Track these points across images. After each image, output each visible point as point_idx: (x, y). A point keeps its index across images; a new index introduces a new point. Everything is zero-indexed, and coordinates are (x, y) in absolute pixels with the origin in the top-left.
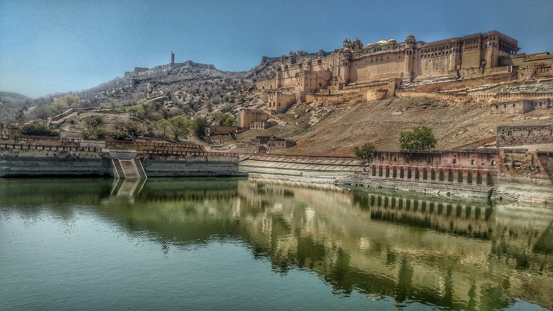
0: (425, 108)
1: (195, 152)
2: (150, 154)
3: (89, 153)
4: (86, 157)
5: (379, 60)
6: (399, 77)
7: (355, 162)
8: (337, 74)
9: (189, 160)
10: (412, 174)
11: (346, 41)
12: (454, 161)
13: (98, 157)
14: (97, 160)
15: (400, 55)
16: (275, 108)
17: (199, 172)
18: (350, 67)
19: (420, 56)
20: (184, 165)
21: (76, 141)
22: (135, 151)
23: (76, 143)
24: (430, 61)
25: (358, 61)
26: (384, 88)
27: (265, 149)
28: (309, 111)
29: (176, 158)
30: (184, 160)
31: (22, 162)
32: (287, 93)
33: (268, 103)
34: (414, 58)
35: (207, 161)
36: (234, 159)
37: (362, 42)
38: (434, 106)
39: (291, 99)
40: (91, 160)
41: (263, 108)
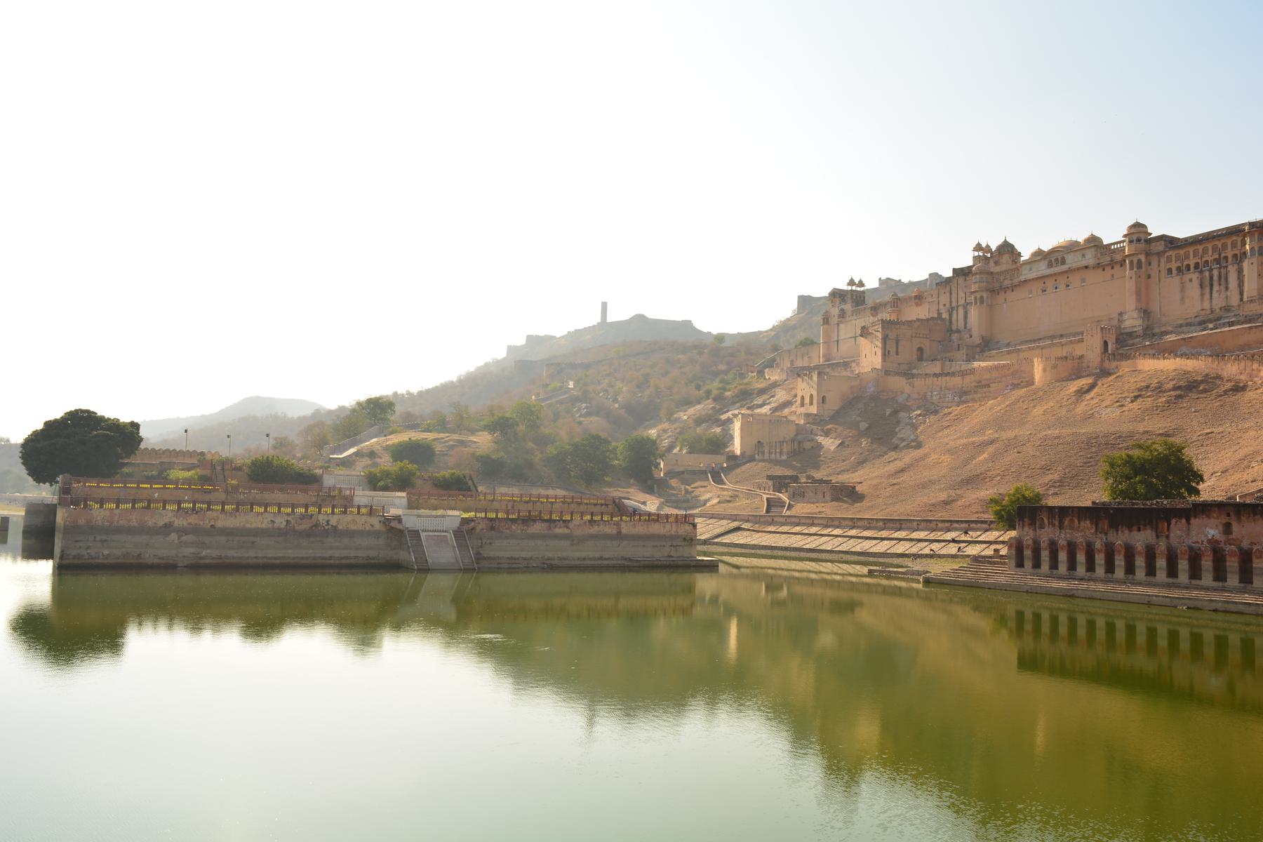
0: (1180, 397)
1: (592, 514)
2: (491, 520)
3: (357, 518)
4: (353, 527)
5: (1062, 286)
6: (1115, 323)
7: (992, 535)
8: (961, 324)
9: (578, 532)
10: (1117, 563)
11: (978, 247)
12: (1227, 529)
13: (378, 526)
14: (376, 534)
15: (1112, 272)
16: (814, 410)
17: (601, 558)
18: (991, 306)
19: (1164, 273)
20: (568, 543)
21: (348, 492)
22: (456, 513)
23: (345, 498)
24: (1191, 280)
25: (1009, 292)
26: (1079, 350)
27: (782, 504)
28: (895, 412)
29: (550, 528)
30: (566, 531)
31: (223, 539)
32: (844, 373)
33: (799, 399)
34: (1149, 277)
35: (619, 533)
36: (684, 529)
37: (1018, 248)
38: (1205, 391)
39: (852, 387)
40: (362, 533)
41: (786, 411)
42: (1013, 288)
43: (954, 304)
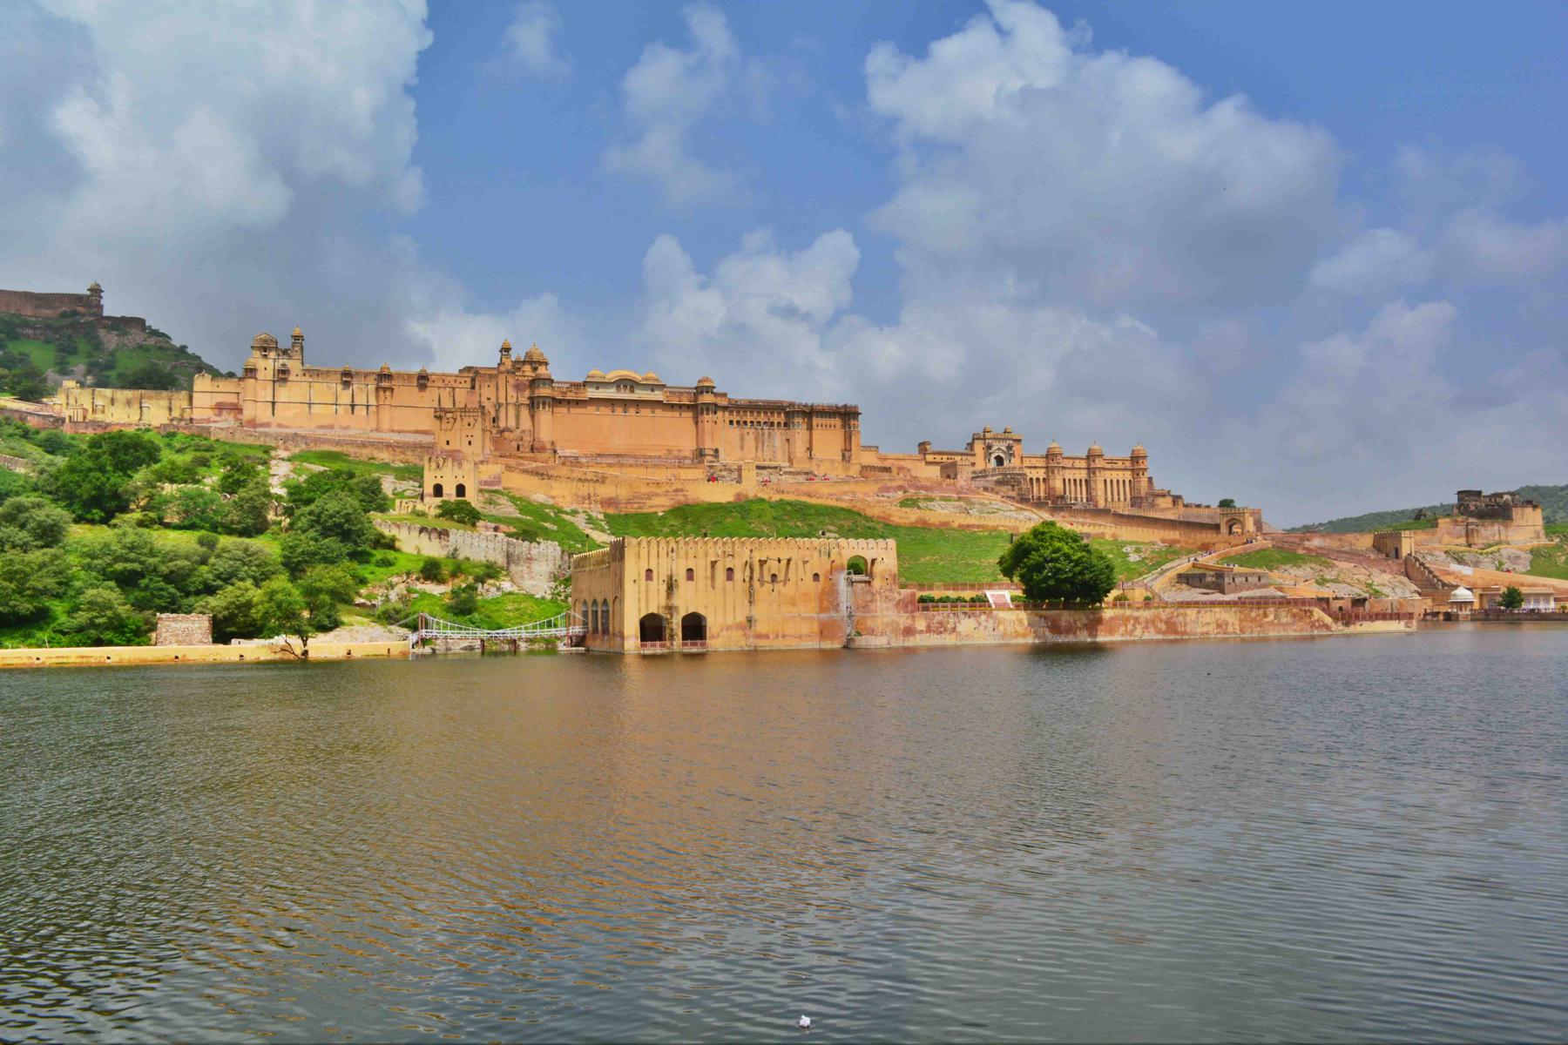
42: (578, 403)
43: (502, 400)
